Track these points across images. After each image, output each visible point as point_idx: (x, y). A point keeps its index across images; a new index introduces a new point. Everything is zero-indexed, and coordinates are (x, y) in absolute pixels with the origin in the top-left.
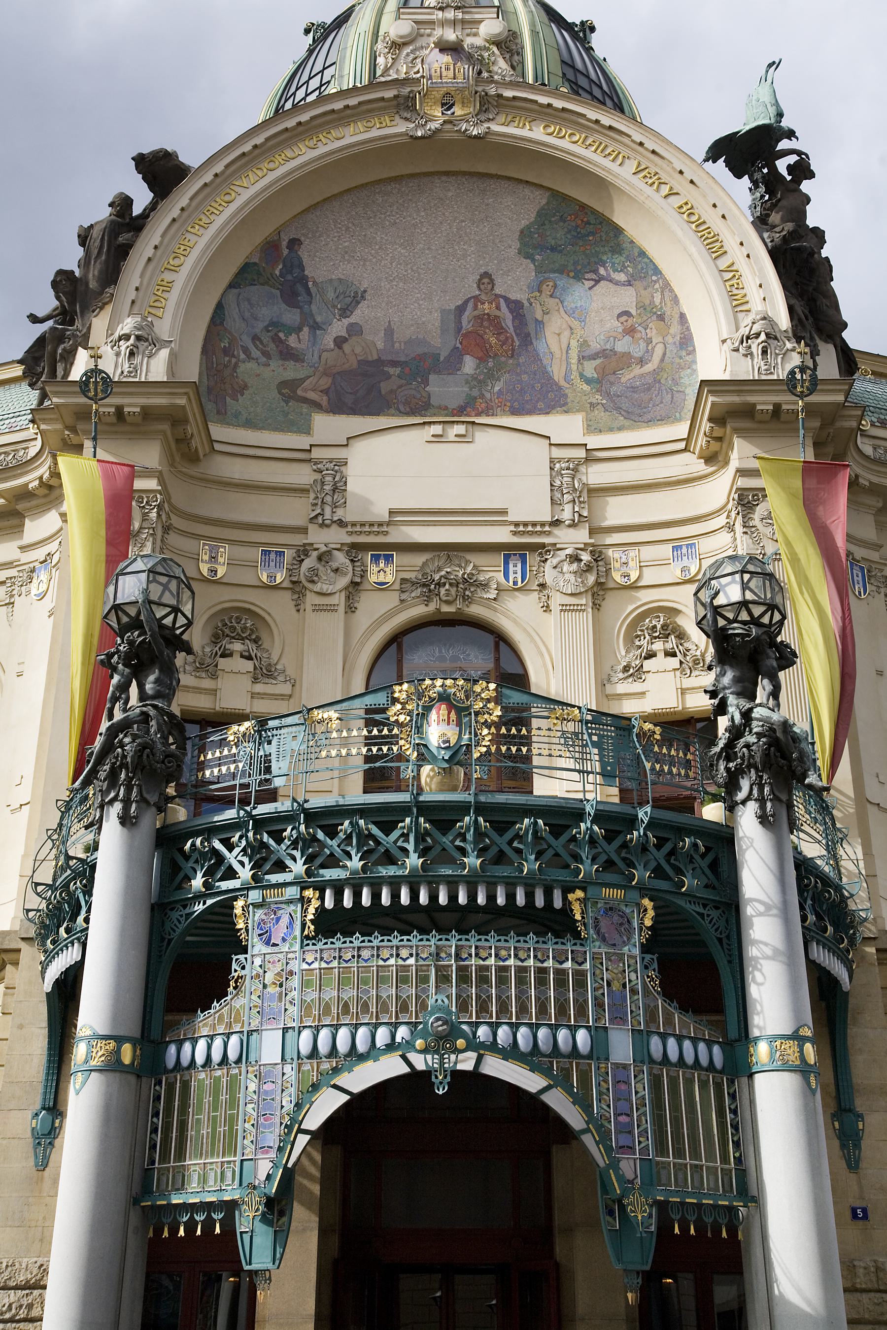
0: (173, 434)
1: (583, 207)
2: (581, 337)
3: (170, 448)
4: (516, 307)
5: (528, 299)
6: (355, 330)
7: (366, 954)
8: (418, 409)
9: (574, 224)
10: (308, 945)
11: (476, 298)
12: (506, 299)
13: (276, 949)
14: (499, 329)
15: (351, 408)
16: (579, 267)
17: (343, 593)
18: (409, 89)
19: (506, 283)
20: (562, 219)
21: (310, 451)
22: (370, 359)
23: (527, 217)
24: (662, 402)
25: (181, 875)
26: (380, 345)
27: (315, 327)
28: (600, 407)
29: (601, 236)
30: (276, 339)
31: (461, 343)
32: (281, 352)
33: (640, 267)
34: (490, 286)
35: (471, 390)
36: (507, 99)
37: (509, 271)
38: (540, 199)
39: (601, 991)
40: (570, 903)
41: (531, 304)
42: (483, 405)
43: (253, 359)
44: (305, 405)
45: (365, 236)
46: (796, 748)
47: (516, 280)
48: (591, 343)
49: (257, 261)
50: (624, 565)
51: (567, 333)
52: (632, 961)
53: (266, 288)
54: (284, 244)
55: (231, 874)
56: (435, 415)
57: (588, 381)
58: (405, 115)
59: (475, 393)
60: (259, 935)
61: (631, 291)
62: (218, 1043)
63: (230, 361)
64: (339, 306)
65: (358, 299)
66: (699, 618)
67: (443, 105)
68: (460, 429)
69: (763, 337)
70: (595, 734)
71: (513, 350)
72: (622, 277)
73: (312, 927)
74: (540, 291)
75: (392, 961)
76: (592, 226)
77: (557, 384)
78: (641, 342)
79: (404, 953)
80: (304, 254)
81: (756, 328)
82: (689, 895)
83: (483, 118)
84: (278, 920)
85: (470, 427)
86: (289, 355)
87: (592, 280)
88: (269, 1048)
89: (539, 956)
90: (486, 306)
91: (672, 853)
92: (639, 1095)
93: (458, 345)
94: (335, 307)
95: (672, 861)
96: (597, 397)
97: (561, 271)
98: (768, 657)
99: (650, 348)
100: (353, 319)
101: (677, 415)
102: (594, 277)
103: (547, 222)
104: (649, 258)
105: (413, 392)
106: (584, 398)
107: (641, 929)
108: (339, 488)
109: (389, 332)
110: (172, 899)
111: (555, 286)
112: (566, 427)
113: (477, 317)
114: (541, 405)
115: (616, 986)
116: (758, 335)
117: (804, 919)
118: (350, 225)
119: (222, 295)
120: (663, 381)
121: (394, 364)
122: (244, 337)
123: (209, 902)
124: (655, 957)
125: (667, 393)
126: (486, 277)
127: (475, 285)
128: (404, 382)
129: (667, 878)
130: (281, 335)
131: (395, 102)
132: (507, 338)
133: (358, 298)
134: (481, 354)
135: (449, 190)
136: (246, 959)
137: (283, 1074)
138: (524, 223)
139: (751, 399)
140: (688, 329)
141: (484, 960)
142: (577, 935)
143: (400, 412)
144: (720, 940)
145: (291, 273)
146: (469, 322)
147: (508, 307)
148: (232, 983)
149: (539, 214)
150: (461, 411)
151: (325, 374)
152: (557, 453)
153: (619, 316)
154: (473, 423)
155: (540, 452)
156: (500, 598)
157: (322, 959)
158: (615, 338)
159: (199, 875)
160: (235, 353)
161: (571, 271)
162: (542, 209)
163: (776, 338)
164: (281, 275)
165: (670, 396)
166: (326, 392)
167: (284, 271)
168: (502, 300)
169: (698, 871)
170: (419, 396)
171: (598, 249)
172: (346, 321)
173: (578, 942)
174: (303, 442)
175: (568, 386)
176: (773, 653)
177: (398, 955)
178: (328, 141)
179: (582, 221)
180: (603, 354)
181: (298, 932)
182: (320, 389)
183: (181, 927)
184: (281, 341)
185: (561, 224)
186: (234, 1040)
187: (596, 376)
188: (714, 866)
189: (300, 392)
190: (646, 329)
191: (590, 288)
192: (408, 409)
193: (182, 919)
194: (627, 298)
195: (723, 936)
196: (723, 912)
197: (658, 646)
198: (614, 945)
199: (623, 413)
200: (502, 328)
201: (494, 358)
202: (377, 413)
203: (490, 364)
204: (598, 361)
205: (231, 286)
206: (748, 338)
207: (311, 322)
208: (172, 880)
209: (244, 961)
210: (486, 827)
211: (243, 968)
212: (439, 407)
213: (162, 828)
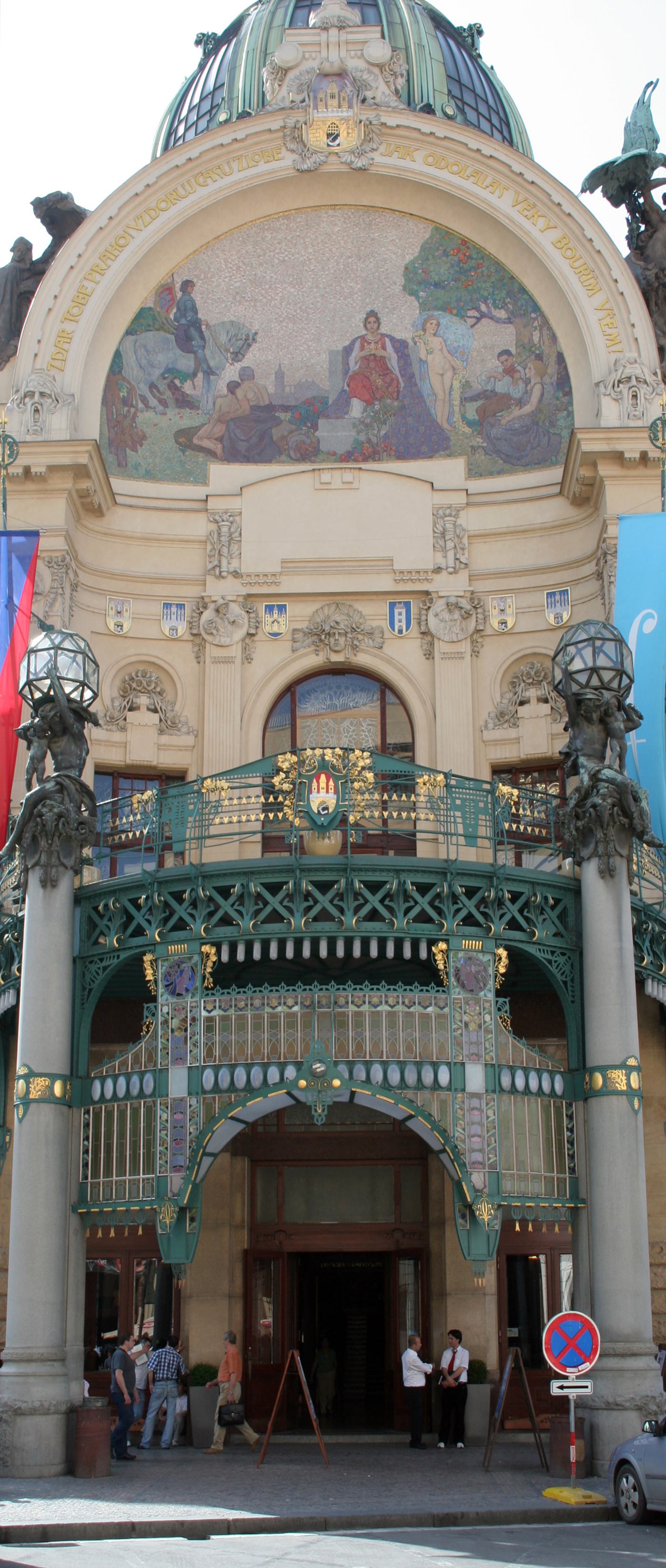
0: (77, 491)
1: (465, 242)
2: (463, 377)
3: (75, 505)
4: (401, 346)
5: (413, 339)
6: (247, 374)
7: (257, 1002)
8: (308, 453)
9: (456, 259)
10: (207, 995)
11: (362, 338)
12: (392, 339)
13: (179, 1000)
14: (385, 370)
15: (245, 456)
16: (462, 304)
17: (240, 644)
18: (294, 120)
19: (391, 321)
20: (445, 253)
21: (207, 500)
22: (262, 404)
23: (412, 253)
24: (539, 445)
25: (97, 931)
26: (271, 389)
27: (209, 372)
28: (480, 450)
29: (482, 272)
30: (172, 387)
31: (348, 386)
32: (177, 400)
33: (519, 304)
34: (376, 325)
35: (358, 434)
36: (391, 128)
37: (394, 309)
38: (424, 233)
39: (459, 1032)
40: (434, 955)
41: (415, 343)
42: (370, 450)
43: (151, 408)
44: (201, 454)
45: (255, 275)
46: (636, 806)
47: (401, 319)
48: (473, 384)
49: (151, 305)
51: (449, 374)
52: (487, 1005)
53: (162, 333)
54: (178, 286)
56: (323, 461)
57: (470, 424)
58: (293, 146)
59: (362, 437)
60: (166, 986)
61: (511, 329)
62: (135, 1079)
63: (129, 411)
64: (231, 350)
65: (250, 341)
66: (556, 682)
67: (329, 135)
68: (348, 476)
69: (634, 382)
70: (459, 798)
71: (398, 392)
72: (502, 314)
73: (211, 980)
74: (424, 330)
75: (279, 1009)
76: (474, 261)
77: (440, 427)
78: (520, 382)
79: (290, 1002)
80: (197, 296)
81: (628, 371)
82: (539, 944)
83: (368, 149)
84: (182, 972)
85: (356, 472)
86: (184, 402)
87: (474, 317)
88: (178, 1083)
89: (407, 1001)
90: (373, 346)
91: (526, 905)
92: (490, 1119)
93: (346, 388)
94: (227, 350)
95: (525, 913)
96: (478, 440)
97: (446, 308)
98: (616, 720)
99: (529, 388)
100: (245, 363)
101: (554, 458)
102: (477, 314)
103: (430, 257)
104: (529, 295)
105: (304, 438)
106: (466, 441)
107: (496, 977)
109: (280, 375)
110: (91, 953)
111: (438, 324)
112: (450, 470)
113: (365, 358)
114: (424, 449)
115: (472, 1026)
116: (629, 378)
117: (639, 959)
118: (241, 264)
119: (120, 343)
120: (540, 423)
121: (286, 408)
122: (142, 386)
123: (124, 955)
124: (507, 1000)
125: (544, 435)
126: (372, 317)
127: (362, 325)
128: (294, 427)
129: (519, 928)
130: (177, 382)
131: (281, 134)
132: (392, 380)
133: (249, 341)
134: (367, 397)
135: (336, 225)
136: (155, 1007)
137: (190, 1106)
138: (409, 258)
139: (619, 447)
140: (566, 368)
141: (358, 1007)
142: (440, 983)
143: (291, 458)
144: (565, 983)
145: (184, 316)
146: (356, 363)
147: (393, 346)
148: (144, 1028)
149: (423, 248)
151: (219, 420)
153: (500, 354)
154: (360, 469)
155: (423, 502)
156: (385, 646)
157: (220, 1007)
158: (495, 378)
159: (113, 932)
160: (134, 402)
161: (454, 308)
162: (426, 243)
163: (645, 382)
164: (176, 319)
165: (546, 438)
166: (220, 440)
167: (178, 314)
168: (387, 340)
169: (548, 922)
170: (308, 441)
171: (479, 285)
172: (238, 366)
173: (441, 989)
174: (199, 492)
175: (450, 428)
176: (620, 716)
177: (285, 1003)
178: (217, 177)
179: (465, 255)
180: (483, 395)
181: (198, 983)
182: (217, 436)
183: (100, 978)
184: (177, 389)
185: (445, 259)
186: (149, 1077)
187: (477, 418)
188: (562, 917)
189: (196, 441)
190: (525, 369)
191: (472, 326)
192: (298, 455)
193: (100, 972)
194: (505, 337)
195: (568, 979)
196: (569, 958)
198: (472, 991)
199: (503, 456)
200: (388, 369)
201: (380, 400)
202: (268, 461)
203: (377, 407)
204: (480, 403)
205: (129, 332)
206: (619, 382)
207: (205, 367)
208: (89, 937)
209: (153, 1009)
210: (360, 888)
211: (153, 1015)
212: (329, 454)
213: (79, 889)
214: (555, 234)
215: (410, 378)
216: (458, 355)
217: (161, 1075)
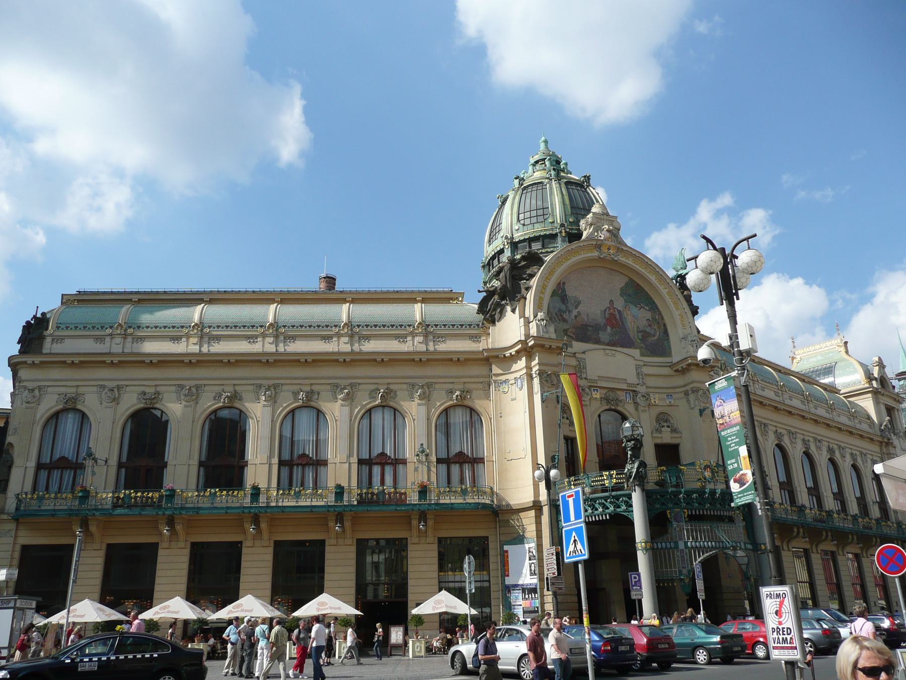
1: (638, 285)
4: (619, 312)
8: (598, 342)
14: (616, 319)
27: (570, 312)
38: (627, 279)
47: (619, 304)
50: (655, 399)
55: (663, 504)
61: (649, 313)
86: (565, 321)
88: (681, 545)
97: (632, 303)
108: (585, 368)
112: (636, 353)
133: (579, 303)
150: (608, 344)
152: (637, 363)
180: (642, 331)
194: (649, 315)
197: (665, 424)
214: (666, 290)
215: (623, 323)
216: (636, 318)
217: (676, 543)
